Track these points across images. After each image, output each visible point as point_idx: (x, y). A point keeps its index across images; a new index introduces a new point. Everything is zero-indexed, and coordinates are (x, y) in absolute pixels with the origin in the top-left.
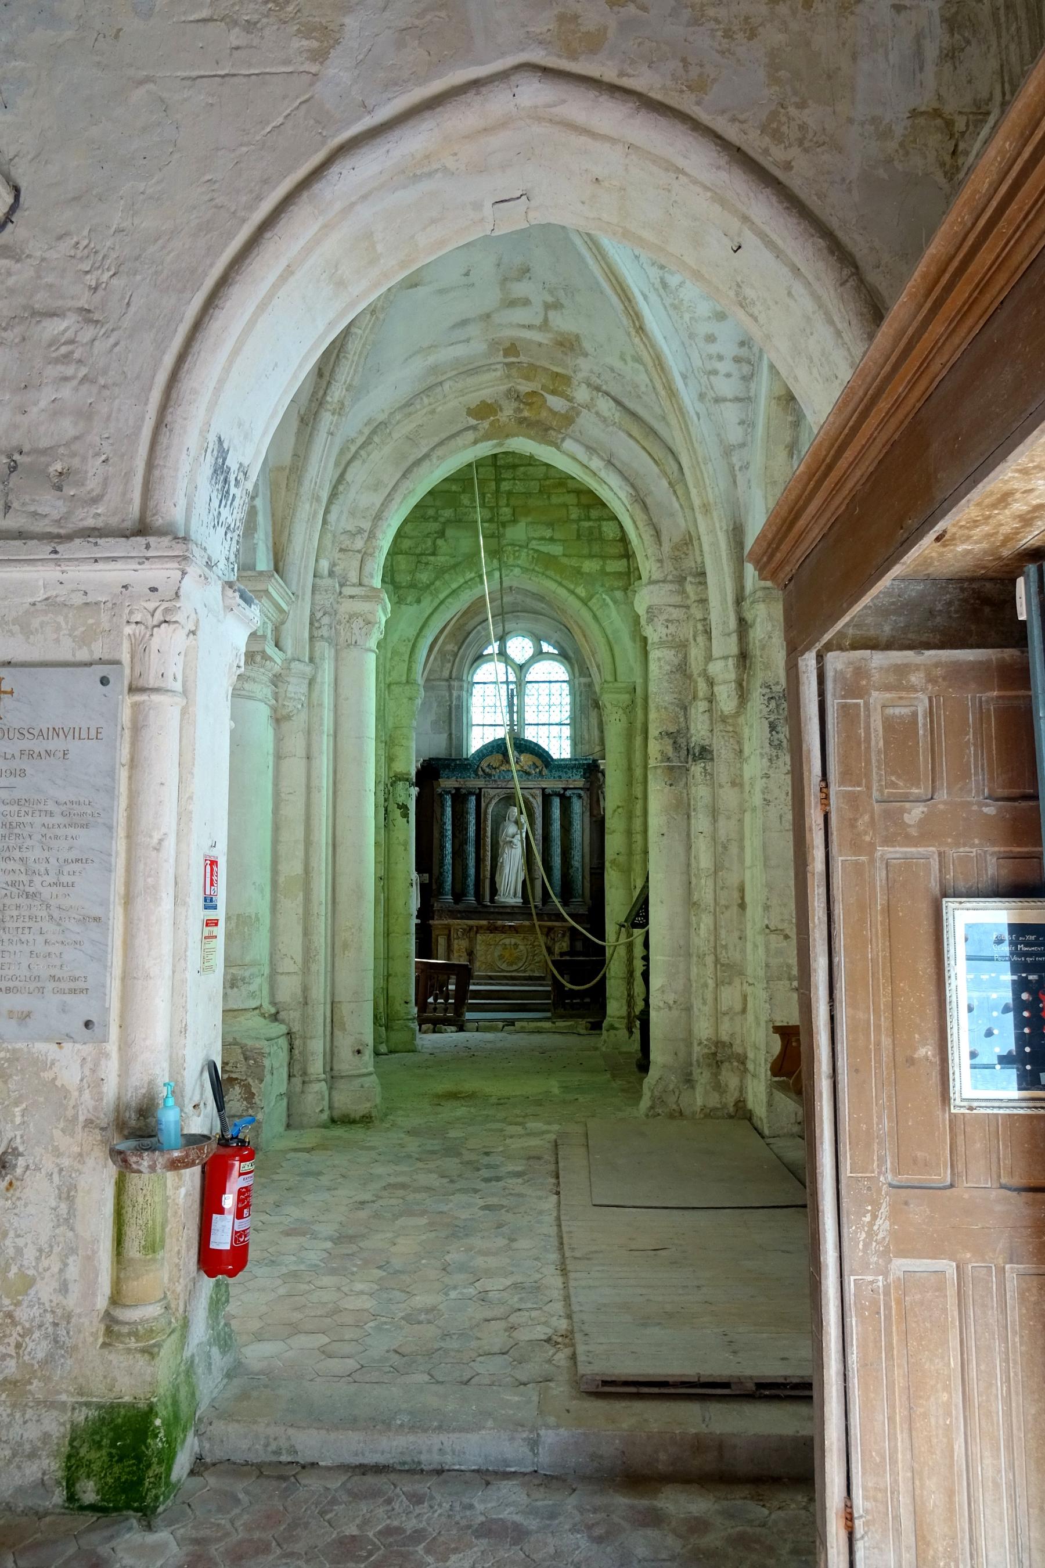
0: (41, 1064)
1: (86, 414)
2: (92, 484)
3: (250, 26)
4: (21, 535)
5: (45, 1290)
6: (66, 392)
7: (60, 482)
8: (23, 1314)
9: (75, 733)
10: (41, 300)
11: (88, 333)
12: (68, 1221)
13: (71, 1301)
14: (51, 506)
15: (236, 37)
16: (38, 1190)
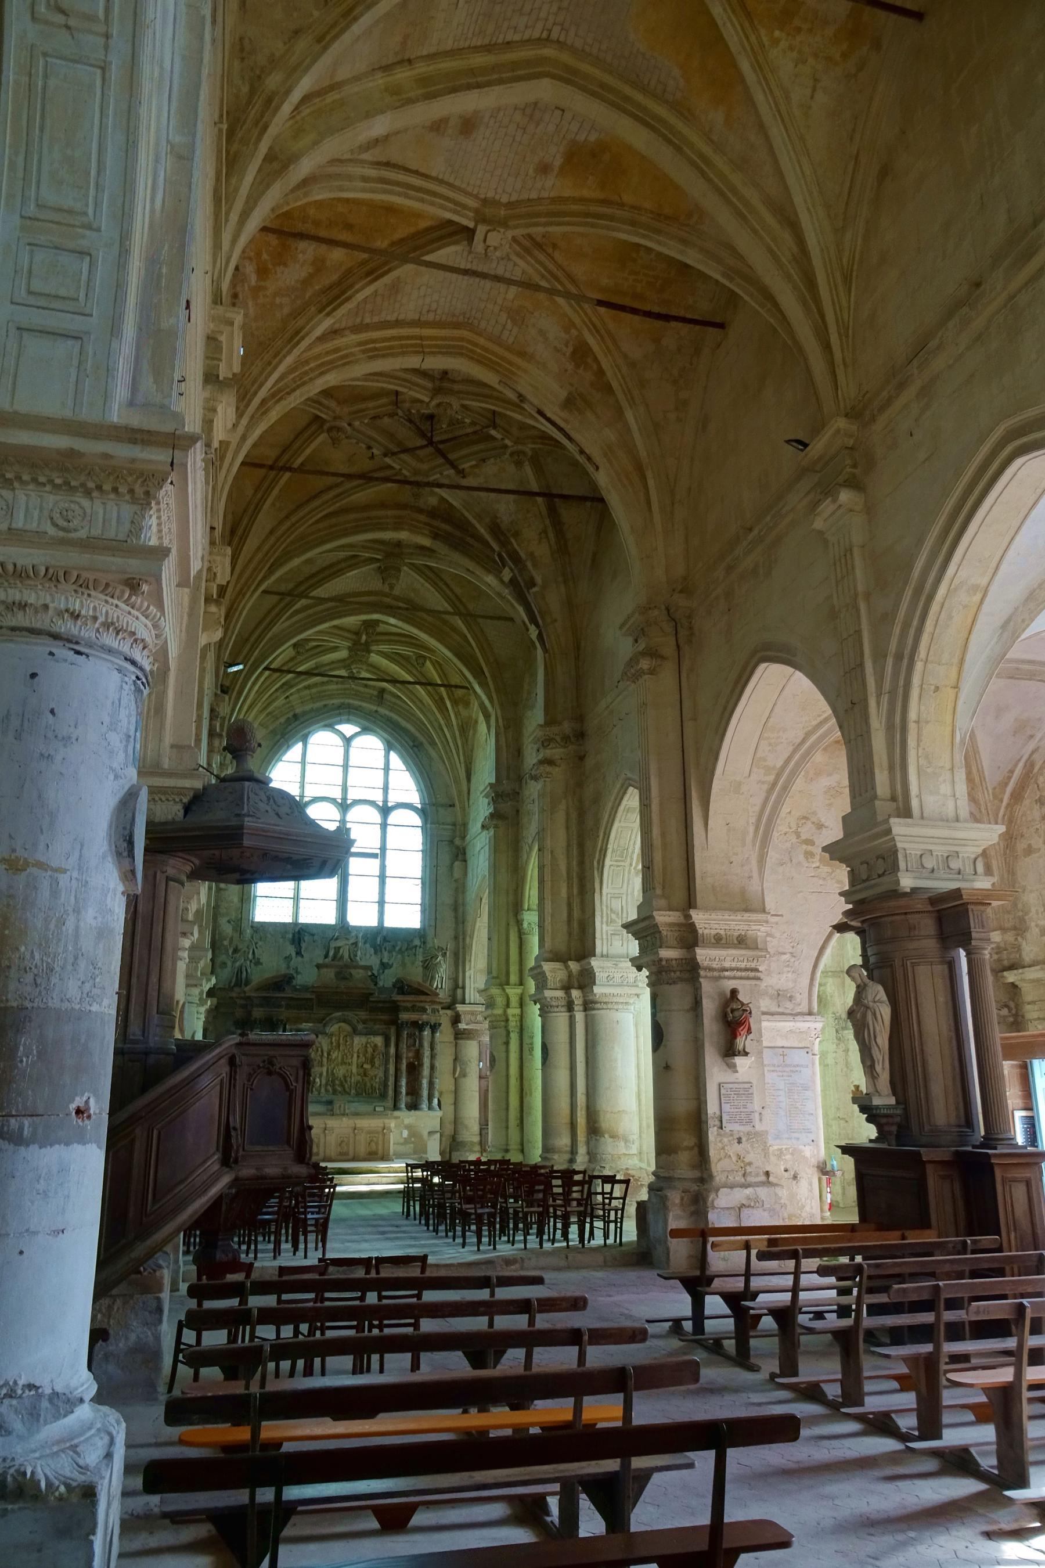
0: (801, 1151)
1: (795, 981)
2: (798, 1000)
3: (824, 879)
4: (783, 1014)
5: (807, 1208)
6: (790, 975)
7: (791, 998)
8: (804, 1215)
9: (802, 1066)
10: (781, 950)
11: (793, 960)
12: (811, 1191)
13: (814, 1211)
14: (789, 1005)
15: (821, 882)
16: (804, 1184)
